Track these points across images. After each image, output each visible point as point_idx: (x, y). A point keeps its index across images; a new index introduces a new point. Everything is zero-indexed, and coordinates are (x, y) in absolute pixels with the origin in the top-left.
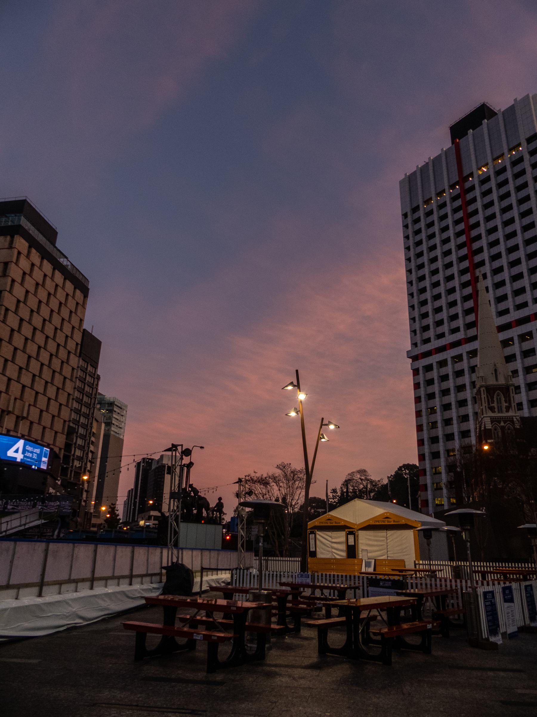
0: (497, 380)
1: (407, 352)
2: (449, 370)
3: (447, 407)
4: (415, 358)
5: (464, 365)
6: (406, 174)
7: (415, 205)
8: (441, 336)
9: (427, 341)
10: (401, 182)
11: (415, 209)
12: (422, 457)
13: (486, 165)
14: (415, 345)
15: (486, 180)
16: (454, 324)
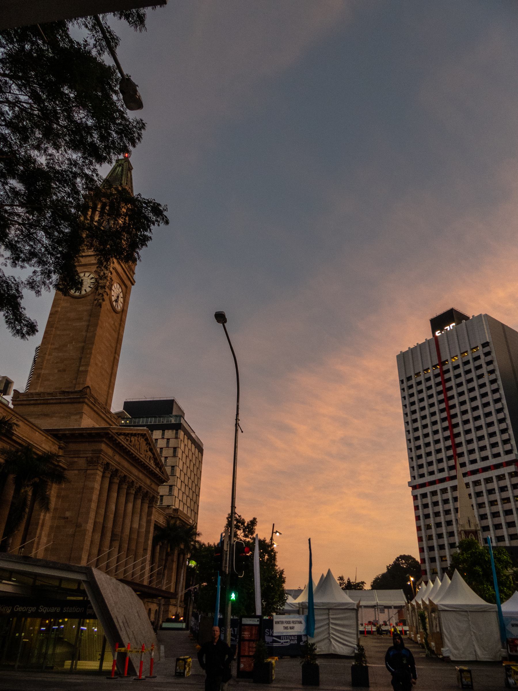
0: (470, 526)
1: (409, 482)
2: (439, 498)
3: (438, 525)
4: (414, 488)
5: (449, 495)
6: (401, 352)
7: (408, 375)
8: (432, 473)
9: (422, 476)
10: (398, 357)
11: (409, 379)
12: (423, 560)
13: (457, 356)
14: (413, 477)
15: (457, 367)
16: (441, 466)
